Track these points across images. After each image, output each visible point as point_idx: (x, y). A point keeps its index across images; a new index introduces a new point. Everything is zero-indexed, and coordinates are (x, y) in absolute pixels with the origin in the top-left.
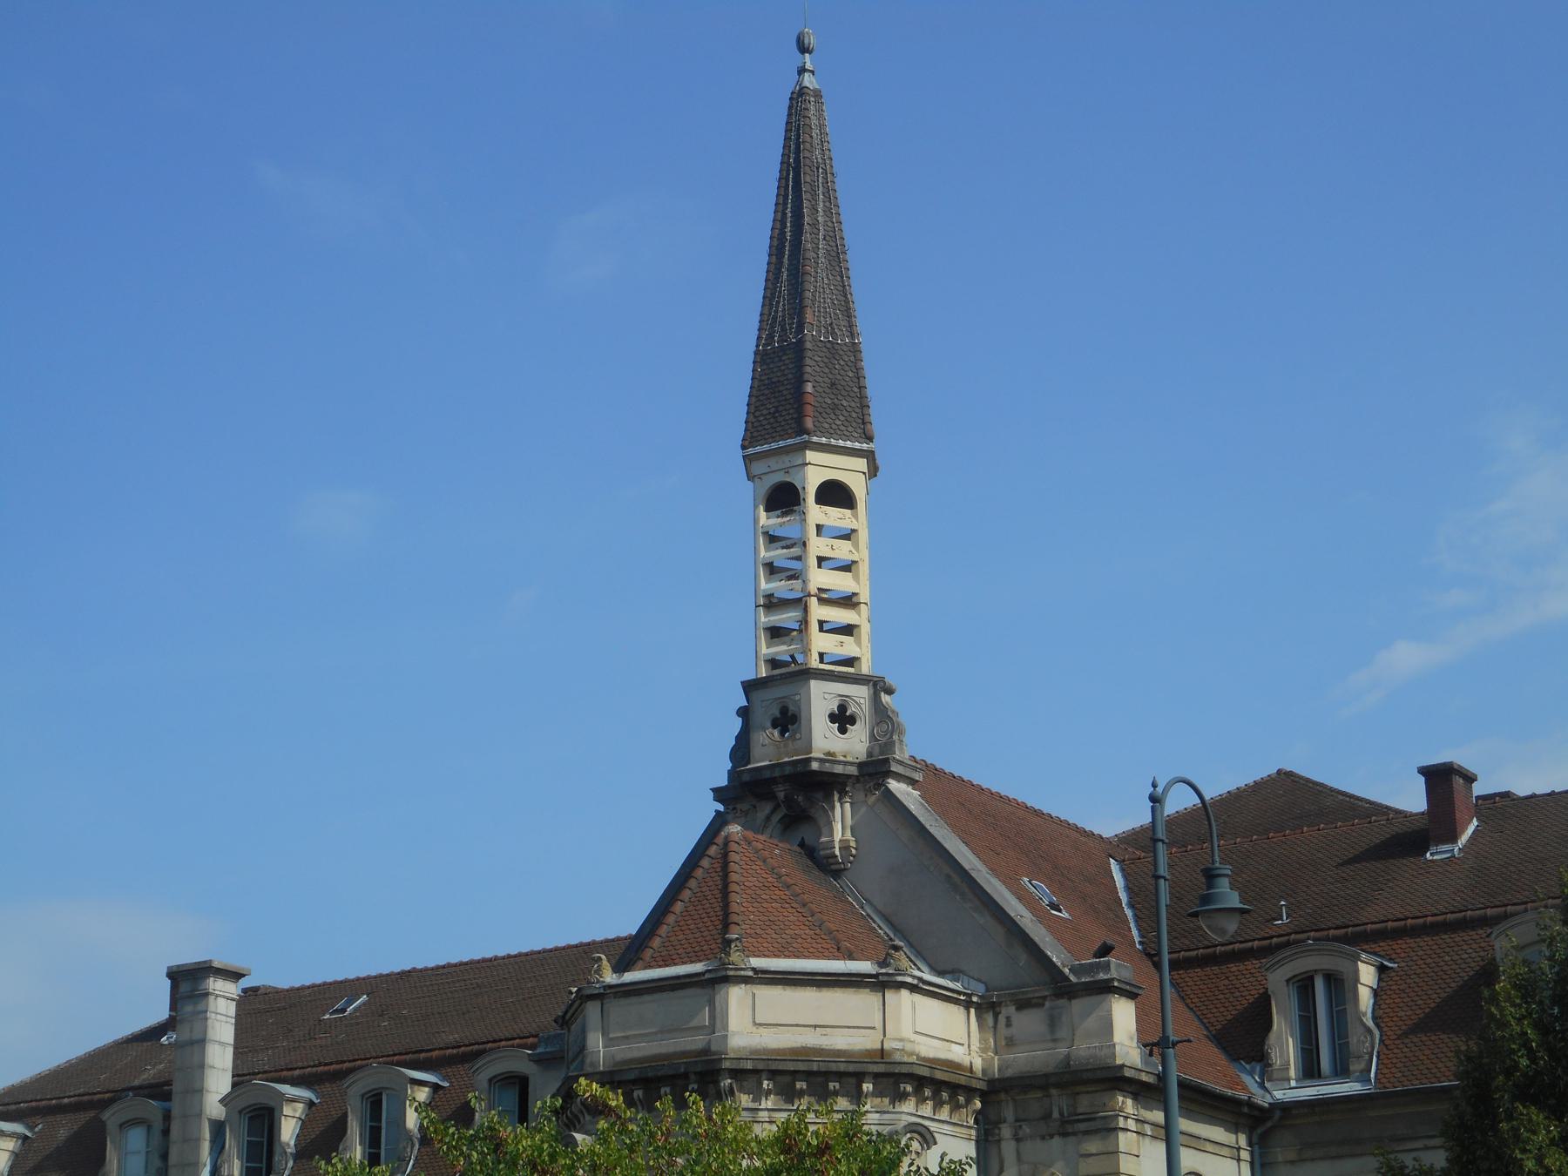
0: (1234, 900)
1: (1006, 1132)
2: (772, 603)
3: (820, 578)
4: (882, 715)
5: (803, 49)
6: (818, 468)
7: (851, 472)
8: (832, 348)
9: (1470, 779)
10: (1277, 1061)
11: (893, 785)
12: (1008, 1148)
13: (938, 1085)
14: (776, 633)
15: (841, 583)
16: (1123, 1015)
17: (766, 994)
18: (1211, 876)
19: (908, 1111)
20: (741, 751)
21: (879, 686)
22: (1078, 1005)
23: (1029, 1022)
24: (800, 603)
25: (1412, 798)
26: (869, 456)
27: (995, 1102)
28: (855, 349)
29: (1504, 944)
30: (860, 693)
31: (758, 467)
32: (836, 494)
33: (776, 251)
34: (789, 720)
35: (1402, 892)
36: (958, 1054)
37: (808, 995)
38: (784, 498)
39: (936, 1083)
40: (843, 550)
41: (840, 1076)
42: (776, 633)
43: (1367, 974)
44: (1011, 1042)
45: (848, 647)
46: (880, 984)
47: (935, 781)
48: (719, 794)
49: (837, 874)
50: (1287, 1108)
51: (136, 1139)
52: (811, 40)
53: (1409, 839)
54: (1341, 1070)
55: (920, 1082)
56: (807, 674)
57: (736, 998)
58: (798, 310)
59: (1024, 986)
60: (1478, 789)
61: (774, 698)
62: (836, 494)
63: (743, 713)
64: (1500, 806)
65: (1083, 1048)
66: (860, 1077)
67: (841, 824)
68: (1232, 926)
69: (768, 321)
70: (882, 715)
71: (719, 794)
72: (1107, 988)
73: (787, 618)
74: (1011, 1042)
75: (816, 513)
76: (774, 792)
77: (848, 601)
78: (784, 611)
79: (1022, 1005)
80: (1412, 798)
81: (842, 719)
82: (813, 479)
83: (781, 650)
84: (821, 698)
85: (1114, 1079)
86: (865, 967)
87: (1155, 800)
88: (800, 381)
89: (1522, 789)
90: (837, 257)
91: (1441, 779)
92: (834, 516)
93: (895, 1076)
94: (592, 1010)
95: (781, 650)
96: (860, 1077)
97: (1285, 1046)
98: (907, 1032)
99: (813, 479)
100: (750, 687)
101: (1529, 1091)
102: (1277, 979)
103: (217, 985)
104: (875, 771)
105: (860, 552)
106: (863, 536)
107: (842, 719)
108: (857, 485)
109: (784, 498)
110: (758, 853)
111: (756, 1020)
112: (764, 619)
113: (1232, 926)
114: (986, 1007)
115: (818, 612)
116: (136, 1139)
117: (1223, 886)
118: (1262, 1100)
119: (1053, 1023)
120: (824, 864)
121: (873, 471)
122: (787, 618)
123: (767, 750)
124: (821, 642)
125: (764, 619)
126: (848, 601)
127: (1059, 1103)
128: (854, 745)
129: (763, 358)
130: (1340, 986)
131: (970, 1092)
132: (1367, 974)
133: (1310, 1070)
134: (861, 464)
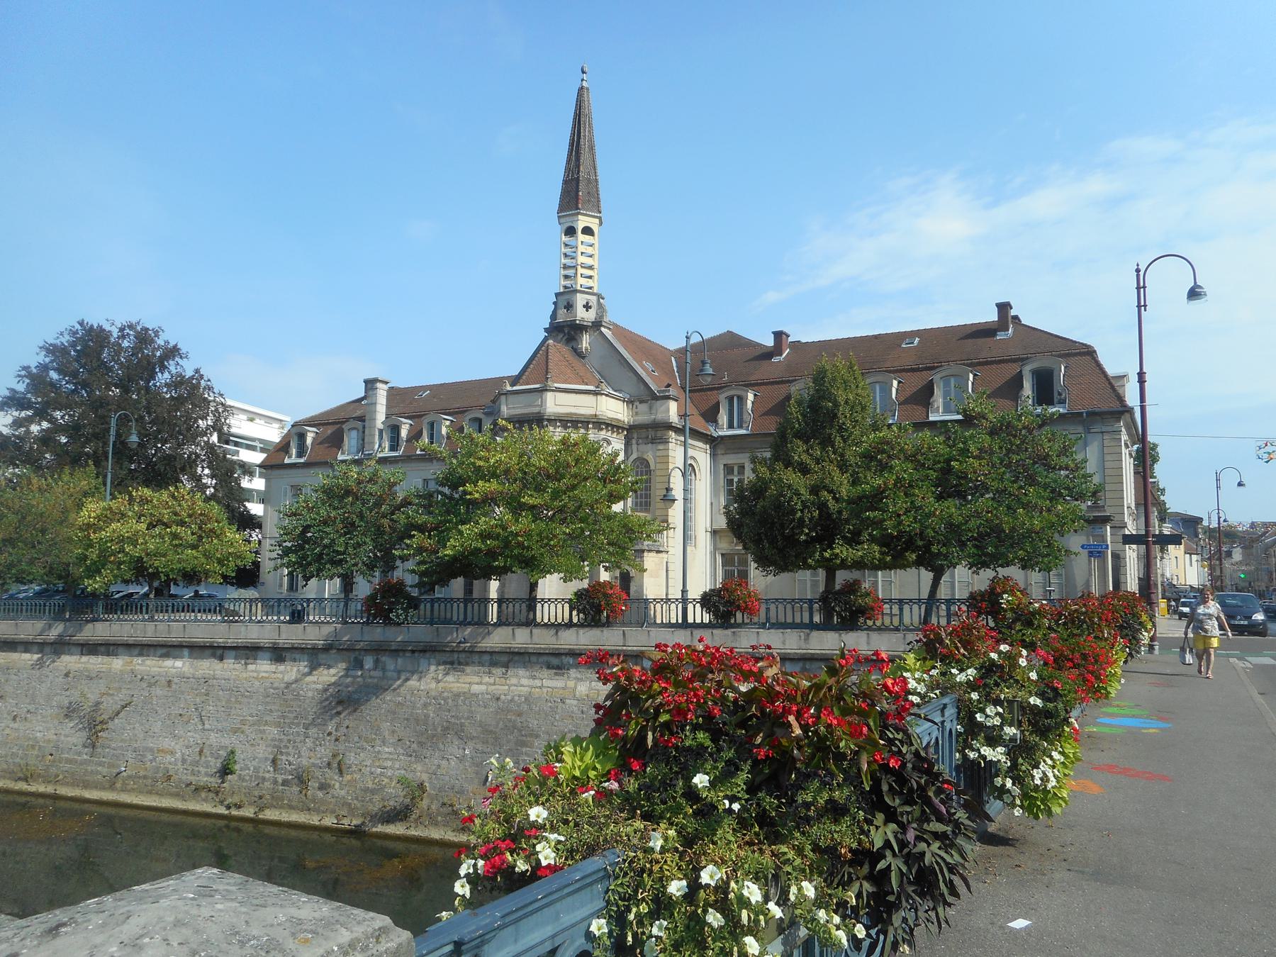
1: (634, 441)
2: (565, 267)
3: (581, 259)
4: (600, 306)
5: (583, 72)
6: (582, 222)
7: (593, 223)
8: (589, 180)
10: (720, 422)
12: (634, 447)
13: (613, 426)
14: (566, 277)
15: (589, 261)
16: (673, 406)
17: (558, 395)
18: (704, 363)
19: (604, 434)
21: (599, 296)
23: (643, 407)
24: (575, 267)
25: (769, 342)
26: (600, 218)
27: (631, 432)
28: (596, 181)
29: (794, 389)
30: (594, 298)
31: (563, 220)
32: (588, 231)
33: (571, 145)
34: (569, 306)
35: (764, 371)
36: (620, 417)
37: (573, 395)
38: (571, 231)
39: (613, 426)
40: (590, 250)
41: (582, 422)
42: (566, 277)
43: (751, 397)
44: (637, 414)
45: (589, 283)
46: (596, 393)
47: (617, 330)
48: (546, 330)
49: (583, 358)
50: (722, 437)
51: (354, 434)
52: (586, 69)
53: (768, 354)
54: (740, 427)
55: (607, 425)
56: (576, 291)
57: (549, 395)
58: (578, 166)
59: (644, 396)
60: (790, 339)
61: (565, 299)
62: (588, 231)
63: (555, 303)
64: (796, 345)
65: (660, 417)
66: (588, 423)
67: (585, 341)
68: (709, 379)
69: (568, 170)
70: (600, 306)
71: (546, 330)
72: (668, 398)
73: (570, 272)
74: (637, 414)
75: (581, 237)
76: (565, 330)
77: (591, 268)
78: (569, 270)
80: (769, 342)
81: (587, 307)
82: (580, 226)
83: (568, 283)
84: (580, 300)
85: (669, 427)
86: (592, 388)
88: (577, 191)
89: (804, 341)
90: (592, 148)
91: (779, 335)
92: (587, 238)
93: (600, 423)
95: (568, 283)
96: (588, 423)
97: (723, 418)
99: (580, 226)
100: (557, 295)
101: (798, 435)
102: (722, 397)
103: (379, 385)
104: (597, 325)
105: (595, 252)
106: (597, 245)
107: (587, 307)
108: (595, 228)
109: (571, 231)
110: (558, 350)
111: (555, 404)
112: (563, 272)
113: (709, 379)
114: (630, 402)
115: (580, 271)
116: (354, 434)
117: (708, 366)
118: (715, 435)
119: (651, 408)
120: (580, 355)
121: (601, 224)
122: (570, 272)
123: (562, 316)
124: (581, 281)
125: (563, 272)
126: (591, 268)
127: (651, 433)
128: (590, 316)
129: (565, 182)
130: (742, 400)
131: (623, 429)
132: (751, 397)
133: (731, 426)
134: (597, 221)
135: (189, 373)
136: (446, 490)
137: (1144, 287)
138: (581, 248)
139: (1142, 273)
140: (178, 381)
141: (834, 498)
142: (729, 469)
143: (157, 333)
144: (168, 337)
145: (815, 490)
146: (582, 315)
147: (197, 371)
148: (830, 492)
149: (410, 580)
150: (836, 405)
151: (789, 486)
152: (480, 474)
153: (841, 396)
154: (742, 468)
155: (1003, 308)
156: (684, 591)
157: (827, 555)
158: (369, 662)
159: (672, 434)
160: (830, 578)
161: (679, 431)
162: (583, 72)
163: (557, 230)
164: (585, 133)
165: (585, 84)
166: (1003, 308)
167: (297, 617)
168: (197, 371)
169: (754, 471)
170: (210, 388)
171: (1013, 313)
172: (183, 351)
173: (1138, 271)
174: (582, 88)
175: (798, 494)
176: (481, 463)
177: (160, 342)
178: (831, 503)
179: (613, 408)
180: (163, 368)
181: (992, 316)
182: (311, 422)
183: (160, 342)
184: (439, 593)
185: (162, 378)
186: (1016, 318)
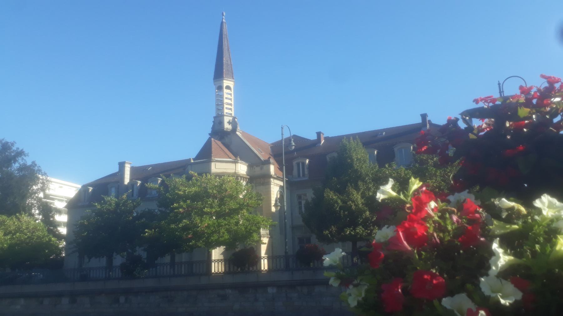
0: (293, 144)
6: (226, 83)
9: (323, 134)
11: (237, 133)
15: (229, 101)
17: (217, 164)
20: (213, 128)
32: (228, 88)
34: (221, 123)
40: (229, 96)
46: (235, 162)
48: (210, 134)
52: (224, 14)
60: (325, 136)
62: (228, 88)
63: (213, 122)
64: (326, 139)
71: (210, 134)
76: (218, 132)
77: (231, 105)
78: (220, 105)
79: (257, 166)
81: (229, 123)
84: (226, 119)
85: (271, 177)
89: (330, 136)
91: (319, 134)
92: (228, 91)
93: (236, 176)
100: (214, 117)
105: (233, 97)
107: (229, 123)
108: (232, 87)
109: (220, 88)
110: (216, 144)
111: (217, 167)
115: (225, 106)
119: (261, 169)
126: (231, 105)
134: (232, 83)
135: (29, 163)
136: (163, 209)
137: (503, 92)
138: (225, 96)
139: (501, 85)
140: (24, 168)
141: (355, 205)
142: (300, 197)
143: (13, 144)
144: (19, 145)
145: (344, 202)
146: (227, 127)
147: (33, 162)
148: (353, 202)
149: (144, 255)
150: (352, 160)
151: (333, 199)
153: (354, 157)
154: (305, 195)
155: (424, 116)
156: (286, 252)
157: (353, 233)
158: (122, 299)
159: (272, 179)
160: (354, 244)
161: (274, 178)
162: (223, 15)
163: (213, 88)
164: (225, 43)
165: (224, 20)
166: (424, 116)
167: (85, 278)
168: (33, 162)
169: (314, 194)
170: (39, 171)
171: (428, 119)
172: (26, 152)
173: (499, 84)
174: (222, 23)
175: (338, 204)
176: (181, 193)
177: (14, 148)
178: (354, 207)
179: (242, 168)
180: (15, 161)
181: (419, 120)
183: (14, 148)
184: (159, 261)
185: (16, 166)
186: (429, 121)
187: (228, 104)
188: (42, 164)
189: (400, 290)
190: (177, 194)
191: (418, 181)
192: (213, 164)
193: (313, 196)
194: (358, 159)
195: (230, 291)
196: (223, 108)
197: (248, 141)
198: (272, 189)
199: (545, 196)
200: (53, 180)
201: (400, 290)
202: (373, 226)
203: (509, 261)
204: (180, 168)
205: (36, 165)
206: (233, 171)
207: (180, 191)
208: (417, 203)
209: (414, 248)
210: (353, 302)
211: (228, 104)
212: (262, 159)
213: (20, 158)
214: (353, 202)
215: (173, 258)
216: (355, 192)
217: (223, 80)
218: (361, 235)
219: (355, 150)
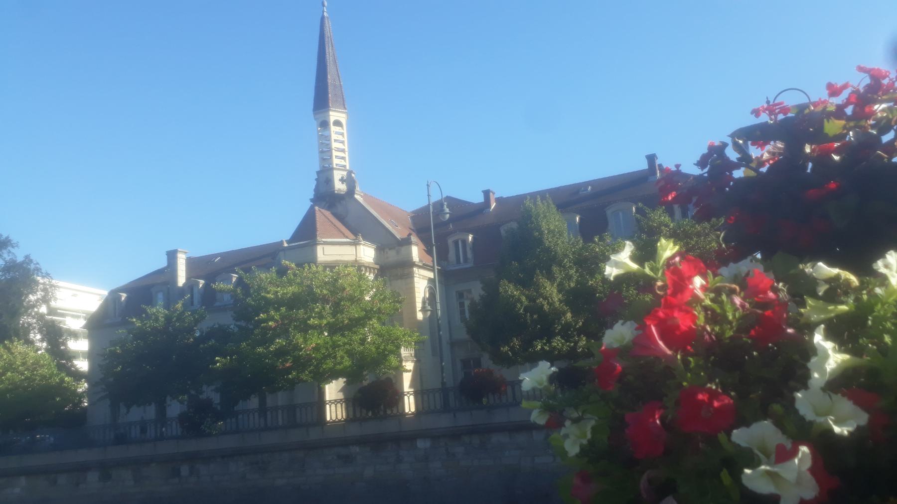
0: (447, 210)
8: (335, 86)
9: (494, 193)
11: (356, 196)
14: (324, 159)
15: (340, 146)
17: (327, 248)
20: (316, 190)
22: (404, 249)
32: (338, 123)
34: (329, 181)
40: (340, 138)
45: (342, 162)
46: (355, 244)
48: (312, 200)
52: (326, 4)
60: (497, 196)
62: (338, 123)
64: (499, 200)
71: (312, 200)
77: (343, 151)
78: (325, 152)
79: (390, 249)
81: (342, 180)
84: (337, 175)
85: (413, 265)
87: (428, 185)
91: (487, 193)
92: (338, 129)
93: (359, 266)
94: (281, 254)
98: (362, 255)
100: (318, 173)
105: (346, 139)
107: (342, 180)
109: (325, 124)
110: (323, 216)
115: (335, 153)
119: (398, 252)
126: (343, 151)
134: (344, 115)
135: (20, 259)
136: (243, 324)
138: (334, 137)
141: (548, 303)
142: (461, 295)
146: (340, 187)
147: (27, 257)
148: (545, 298)
149: (216, 398)
150: (541, 233)
152: (268, 304)
153: (544, 226)
154: (470, 291)
155: (651, 159)
156: (443, 383)
157: (547, 348)
158: (185, 470)
161: (419, 267)
162: (324, 6)
164: (329, 50)
166: (651, 159)
167: (121, 440)
169: (483, 289)
170: (38, 270)
171: (658, 162)
172: (14, 241)
174: (323, 18)
175: (521, 303)
176: (271, 296)
178: (546, 307)
179: (367, 253)
181: (644, 165)
182: (123, 289)
184: (241, 406)
186: (660, 165)
187: (338, 150)
188: (41, 259)
189: (658, 422)
190: (265, 298)
191: (671, 245)
192: (319, 249)
193: (482, 293)
194: (550, 231)
195: (356, 449)
196: (331, 156)
197: (374, 209)
198: (416, 285)
199: (891, 255)
200: (61, 284)
201: (658, 422)
202: (579, 336)
203: (843, 361)
204: (266, 256)
205: (31, 261)
206: (353, 258)
207: (268, 293)
208: (675, 278)
209: (676, 352)
210: (572, 448)
211: (338, 150)
212: (398, 237)
213: (4, 251)
214: (545, 298)
215: (263, 401)
216: (547, 284)
217: (328, 111)
218: (559, 351)
219: (545, 217)
